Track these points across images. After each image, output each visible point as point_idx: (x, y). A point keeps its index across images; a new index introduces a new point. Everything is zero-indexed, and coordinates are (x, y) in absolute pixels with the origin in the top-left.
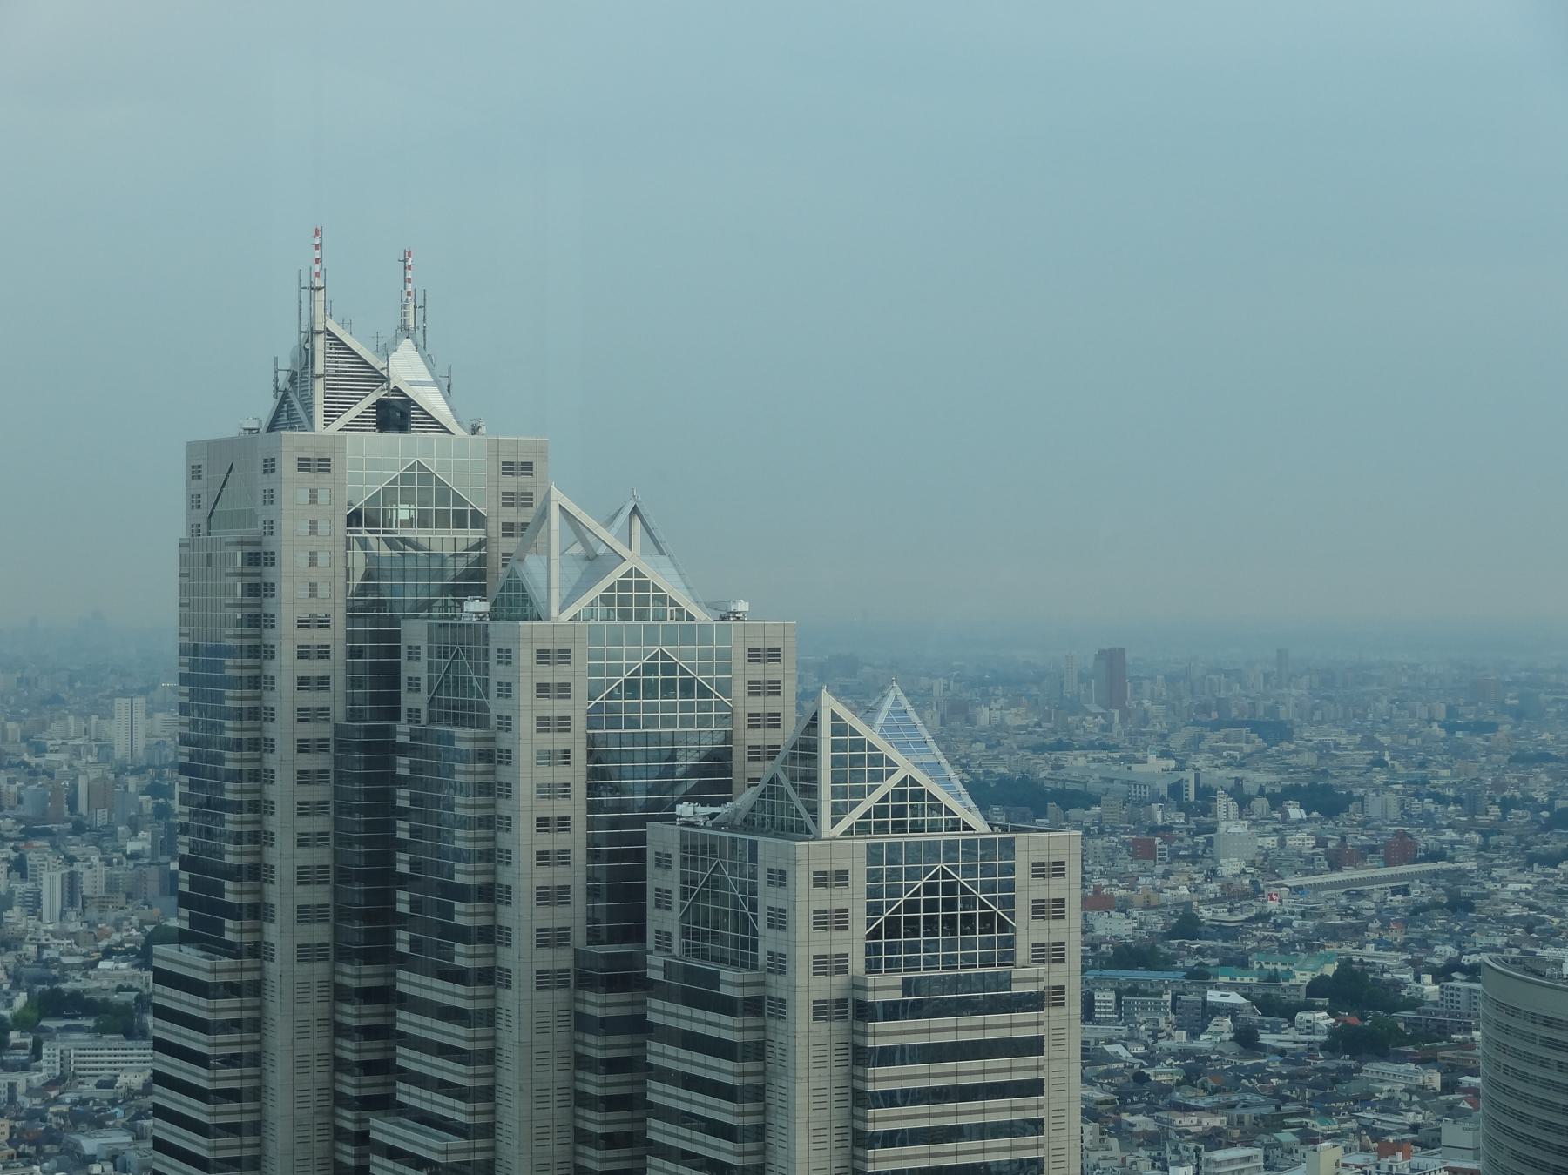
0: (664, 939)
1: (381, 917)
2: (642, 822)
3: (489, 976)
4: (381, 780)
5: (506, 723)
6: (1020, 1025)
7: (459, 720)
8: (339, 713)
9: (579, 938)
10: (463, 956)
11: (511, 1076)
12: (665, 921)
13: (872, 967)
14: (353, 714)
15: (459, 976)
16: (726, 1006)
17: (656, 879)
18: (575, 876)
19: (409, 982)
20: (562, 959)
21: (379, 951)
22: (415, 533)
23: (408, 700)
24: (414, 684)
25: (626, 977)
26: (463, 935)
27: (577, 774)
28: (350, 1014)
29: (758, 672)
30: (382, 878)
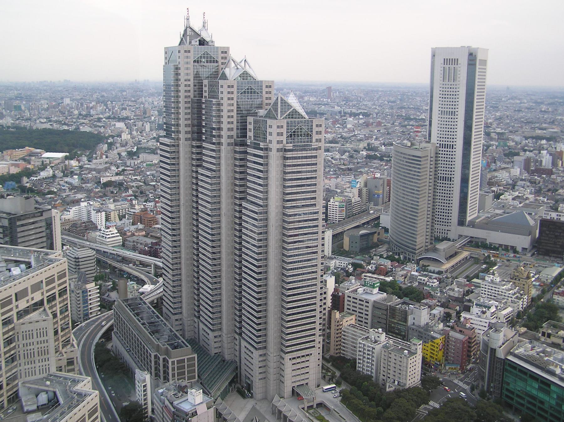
0: (250, 137)
1: (200, 133)
2: (246, 117)
3: (219, 144)
4: (200, 108)
5: (222, 99)
6: (314, 153)
7: (213, 98)
8: (192, 96)
9: (235, 137)
10: (214, 140)
11: (223, 162)
12: (250, 134)
13: (287, 143)
14: (194, 97)
15: (214, 144)
16: (261, 149)
17: (249, 127)
18: (234, 126)
19: (204, 145)
20: (232, 141)
21: (200, 139)
22: (205, 64)
23: (204, 94)
24: (206, 92)
25: (243, 144)
26: (214, 136)
27: (235, 108)
28: (194, 150)
29: (267, 90)
30: (200, 126)
